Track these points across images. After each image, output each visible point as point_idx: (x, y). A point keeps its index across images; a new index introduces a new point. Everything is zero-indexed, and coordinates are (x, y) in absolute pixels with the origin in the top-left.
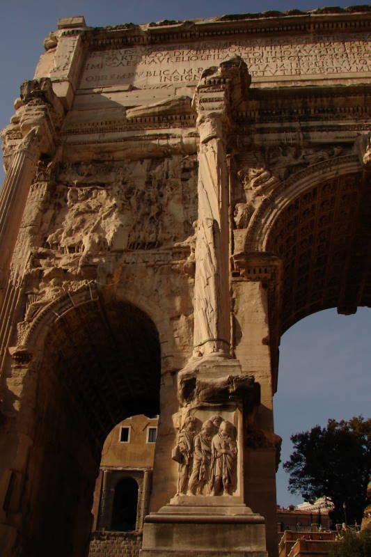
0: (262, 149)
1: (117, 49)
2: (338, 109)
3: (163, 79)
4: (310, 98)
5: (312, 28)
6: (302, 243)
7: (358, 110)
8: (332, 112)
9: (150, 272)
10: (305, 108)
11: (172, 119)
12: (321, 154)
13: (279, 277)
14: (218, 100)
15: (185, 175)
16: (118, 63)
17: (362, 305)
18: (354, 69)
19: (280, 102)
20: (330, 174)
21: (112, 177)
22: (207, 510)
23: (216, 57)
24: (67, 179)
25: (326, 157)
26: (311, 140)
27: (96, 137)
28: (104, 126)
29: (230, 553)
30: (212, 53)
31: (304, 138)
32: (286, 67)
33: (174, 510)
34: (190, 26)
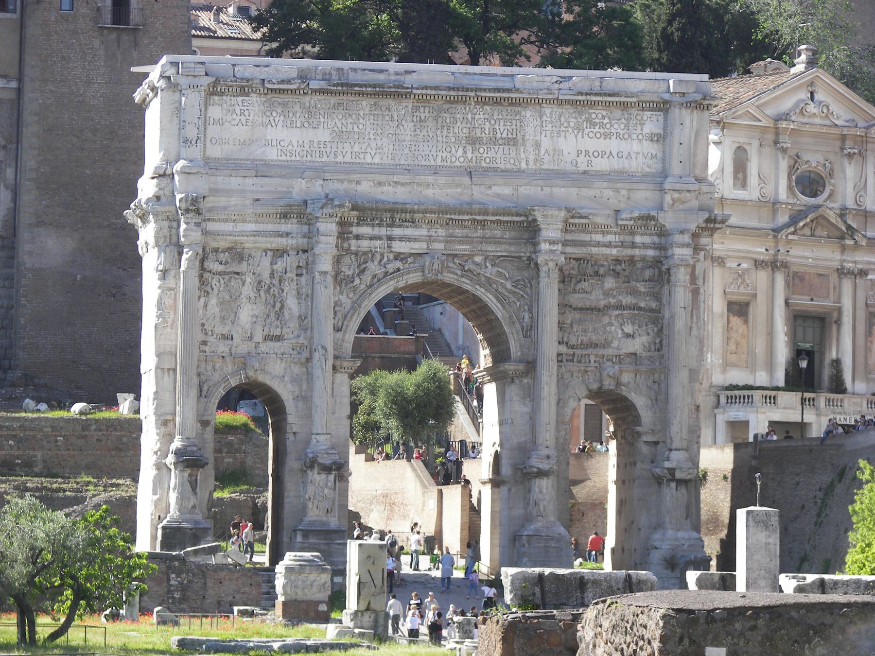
0: (356, 254)
1: (234, 96)
3: (279, 150)
9: (279, 361)
10: (392, 218)
12: (398, 264)
16: (237, 120)
18: (439, 159)
19: (374, 213)
21: (243, 267)
24: (211, 267)
26: (393, 250)
27: (228, 227)
28: (236, 217)
30: (322, 120)
31: (388, 247)
32: (385, 150)
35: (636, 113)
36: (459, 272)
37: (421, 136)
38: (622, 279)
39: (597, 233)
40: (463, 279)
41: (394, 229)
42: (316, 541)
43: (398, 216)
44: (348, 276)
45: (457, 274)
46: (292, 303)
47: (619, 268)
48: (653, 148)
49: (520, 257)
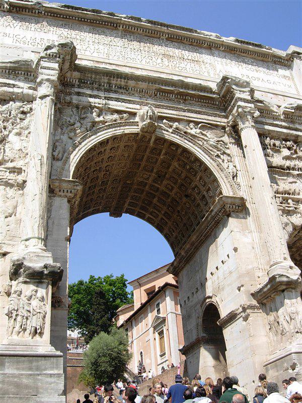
0: (77, 107)
2: (130, 88)
3: (15, 40)
4: (114, 77)
5: (121, 27)
6: (94, 171)
7: (142, 91)
8: (126, 89)
10: (109, 84)
11: (18, 73)
12: (116, 116)
13: (78, 196)
14: (53, 69)
15: (22, 116)
17: (126, 212)
20: (119, 131)
22: (23, 348)
23: (54, 32)
25: (118, 119)
29: (40, 374)
31: (106, 104)
32: (101, 51)
33: (6, 348)
34: (39, 6)
35: (271, 64)
36: (171, 130)
37: (129, 49)
38: (293, 151)
39: (269, 118)
40: (173, 135)
41: (110, 93)
42: (16, 372)
43: (114, 82)
44: (69, 121)
45: (167, 131)
46: (12, 138)
47: (288, 143)
48: (289, 83)
49: (217, 126)
